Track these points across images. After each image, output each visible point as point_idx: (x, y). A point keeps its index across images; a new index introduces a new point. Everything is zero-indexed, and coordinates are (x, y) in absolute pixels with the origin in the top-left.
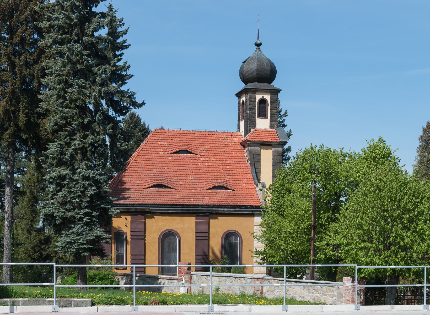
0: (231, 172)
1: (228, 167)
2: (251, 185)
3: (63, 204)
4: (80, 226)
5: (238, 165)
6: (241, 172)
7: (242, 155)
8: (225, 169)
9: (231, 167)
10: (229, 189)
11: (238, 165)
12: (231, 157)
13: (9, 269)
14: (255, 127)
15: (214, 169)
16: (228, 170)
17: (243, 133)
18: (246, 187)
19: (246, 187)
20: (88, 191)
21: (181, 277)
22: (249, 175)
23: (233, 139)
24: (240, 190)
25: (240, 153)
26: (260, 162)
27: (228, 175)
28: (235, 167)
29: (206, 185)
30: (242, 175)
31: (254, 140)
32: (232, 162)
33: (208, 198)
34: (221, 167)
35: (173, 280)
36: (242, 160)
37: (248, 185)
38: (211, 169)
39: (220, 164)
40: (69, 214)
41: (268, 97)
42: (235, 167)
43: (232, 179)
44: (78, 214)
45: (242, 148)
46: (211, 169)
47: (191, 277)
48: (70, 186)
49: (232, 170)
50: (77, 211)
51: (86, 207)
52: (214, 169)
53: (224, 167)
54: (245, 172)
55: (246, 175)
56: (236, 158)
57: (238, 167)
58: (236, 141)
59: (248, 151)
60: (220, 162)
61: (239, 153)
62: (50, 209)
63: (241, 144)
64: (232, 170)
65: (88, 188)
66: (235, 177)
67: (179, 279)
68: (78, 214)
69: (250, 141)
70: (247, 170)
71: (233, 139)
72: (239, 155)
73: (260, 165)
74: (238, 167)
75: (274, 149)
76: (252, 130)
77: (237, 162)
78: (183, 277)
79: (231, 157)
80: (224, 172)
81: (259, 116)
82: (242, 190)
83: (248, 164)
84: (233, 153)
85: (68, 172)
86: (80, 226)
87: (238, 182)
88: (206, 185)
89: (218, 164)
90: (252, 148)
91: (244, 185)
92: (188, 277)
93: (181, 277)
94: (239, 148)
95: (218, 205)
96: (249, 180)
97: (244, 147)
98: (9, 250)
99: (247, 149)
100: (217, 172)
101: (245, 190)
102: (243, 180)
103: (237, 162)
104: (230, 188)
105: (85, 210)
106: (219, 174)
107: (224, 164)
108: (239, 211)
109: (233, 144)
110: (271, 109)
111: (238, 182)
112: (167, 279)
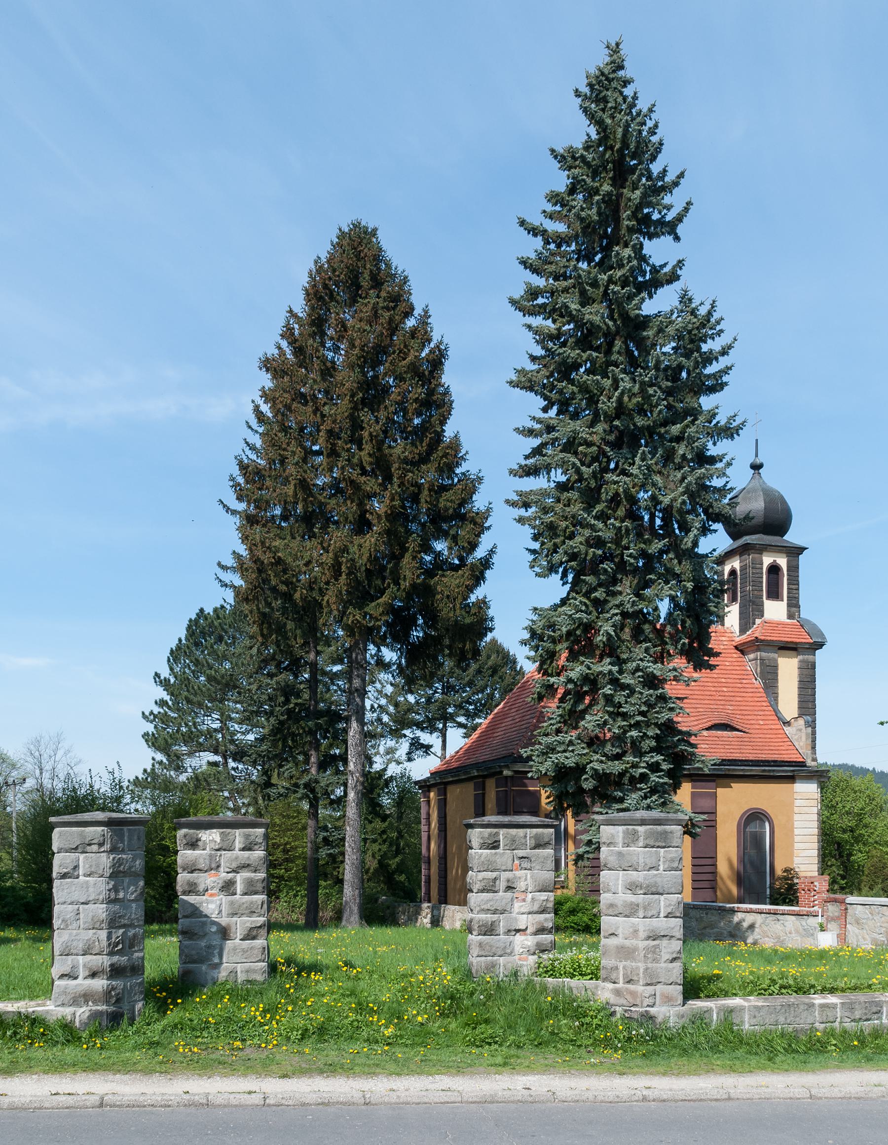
0: (732, 698)
1: (725, 689)
2: (771, 722)
3: (593, 742)
4: (641, 793)
5: (740, 685)
6: (751, 699)
7: (743, 668)
8: (721, 694)
9: (730, 689)
10: (738, 730)
11: (740, 685)
12: (725, 672)
13: (357, 892)
14: (763, 616)
15: (702, 693)
16: (727, 694)
17: (736, 628)
18: (766, 727)
19: (766, 727)
20: (656, 712)
21: (812, 909)
22: (764, 704)
23: (721, 638)
24: (757, 731)
25: (739, 664)
26: (776, 679)
27: (728, 703)
28: (737, 690)
29: (696, 723)
30: (752, 704)
31: (769, 638)
32: (729, 680)
33: (707, 746)
34: (713, 689)
35: (783, 914)
36: (745, 677)
37: (767, 722)
38: (696, 692)
39: (710, 684)
40: (616, 767)
41: (783, 562)
42: (737, 690)
43: (739, 712)
44: (635, 766)
45: (739, 654)
46: (696, 692)
47: (846, 909)
48: (616, 699)
49: (733, 694)
50: (630, 758)
51: (652, 750)
52: (702, 693)
53: (719, 689)
54: (757, 699)
55: (759, 704)
56: (734, 672)
57: (742, 690)
58: (725, 643)
59: (756, 659)
60: (709, 680)
61: (736, 664)
62: (567, 754)
63: (736, 647)
64: (733, 694)
65: (656, 704)
66: (742, 708)
67: (805, 913)
68: (635, 766)
69: (762, 641)
70: (759, 695)
71: (721, 638)
72: (738, 668)
73: (777, 687)
74: (742, 690)
75: (801, 657)
76: (758, 621)
77: (738, 681)
78: (816, 908)
79: (725, 672)
80: (720, 698)
81: (769, 597)
82: (760, 731)
83: (758, 683)
84: (727, 664)
85: (605, 666)
86: (641, 793)
87: (750, 717)
88: (696, 723)
89: (706, 684)
90: (764, 654)
91: (761, 722)
92: (837, 909)
93: (812, 909)
94: (735, 655)
95: (729, 760)
96: (767, 713)
97: (743, 652)
98: (358, 851)
99: (752, 656)
100: (708, 697)
101: (765, 732)
102: (756, 713)
103: (738, 681)
104: (741, 728)
105: (652, 757)
106: (712, 702)
107: (716, 684)
108: (770, 771)
109: (722, 647)
110: (788, 584)
111: (750, 717)
112: (761, 913)
